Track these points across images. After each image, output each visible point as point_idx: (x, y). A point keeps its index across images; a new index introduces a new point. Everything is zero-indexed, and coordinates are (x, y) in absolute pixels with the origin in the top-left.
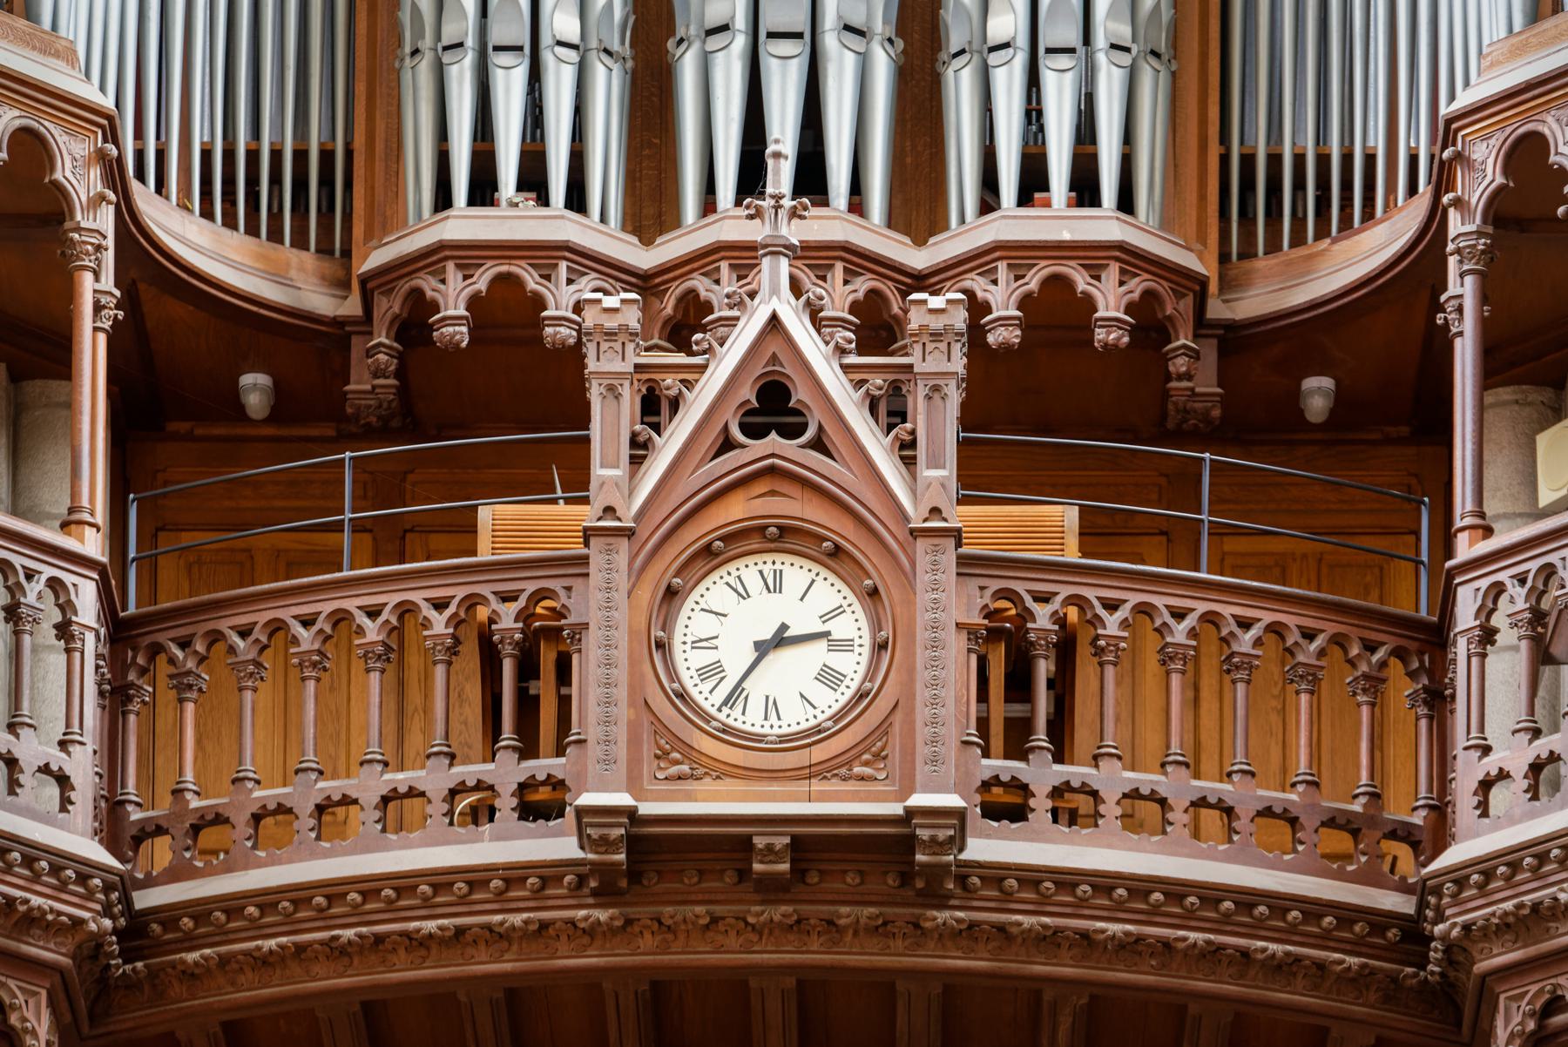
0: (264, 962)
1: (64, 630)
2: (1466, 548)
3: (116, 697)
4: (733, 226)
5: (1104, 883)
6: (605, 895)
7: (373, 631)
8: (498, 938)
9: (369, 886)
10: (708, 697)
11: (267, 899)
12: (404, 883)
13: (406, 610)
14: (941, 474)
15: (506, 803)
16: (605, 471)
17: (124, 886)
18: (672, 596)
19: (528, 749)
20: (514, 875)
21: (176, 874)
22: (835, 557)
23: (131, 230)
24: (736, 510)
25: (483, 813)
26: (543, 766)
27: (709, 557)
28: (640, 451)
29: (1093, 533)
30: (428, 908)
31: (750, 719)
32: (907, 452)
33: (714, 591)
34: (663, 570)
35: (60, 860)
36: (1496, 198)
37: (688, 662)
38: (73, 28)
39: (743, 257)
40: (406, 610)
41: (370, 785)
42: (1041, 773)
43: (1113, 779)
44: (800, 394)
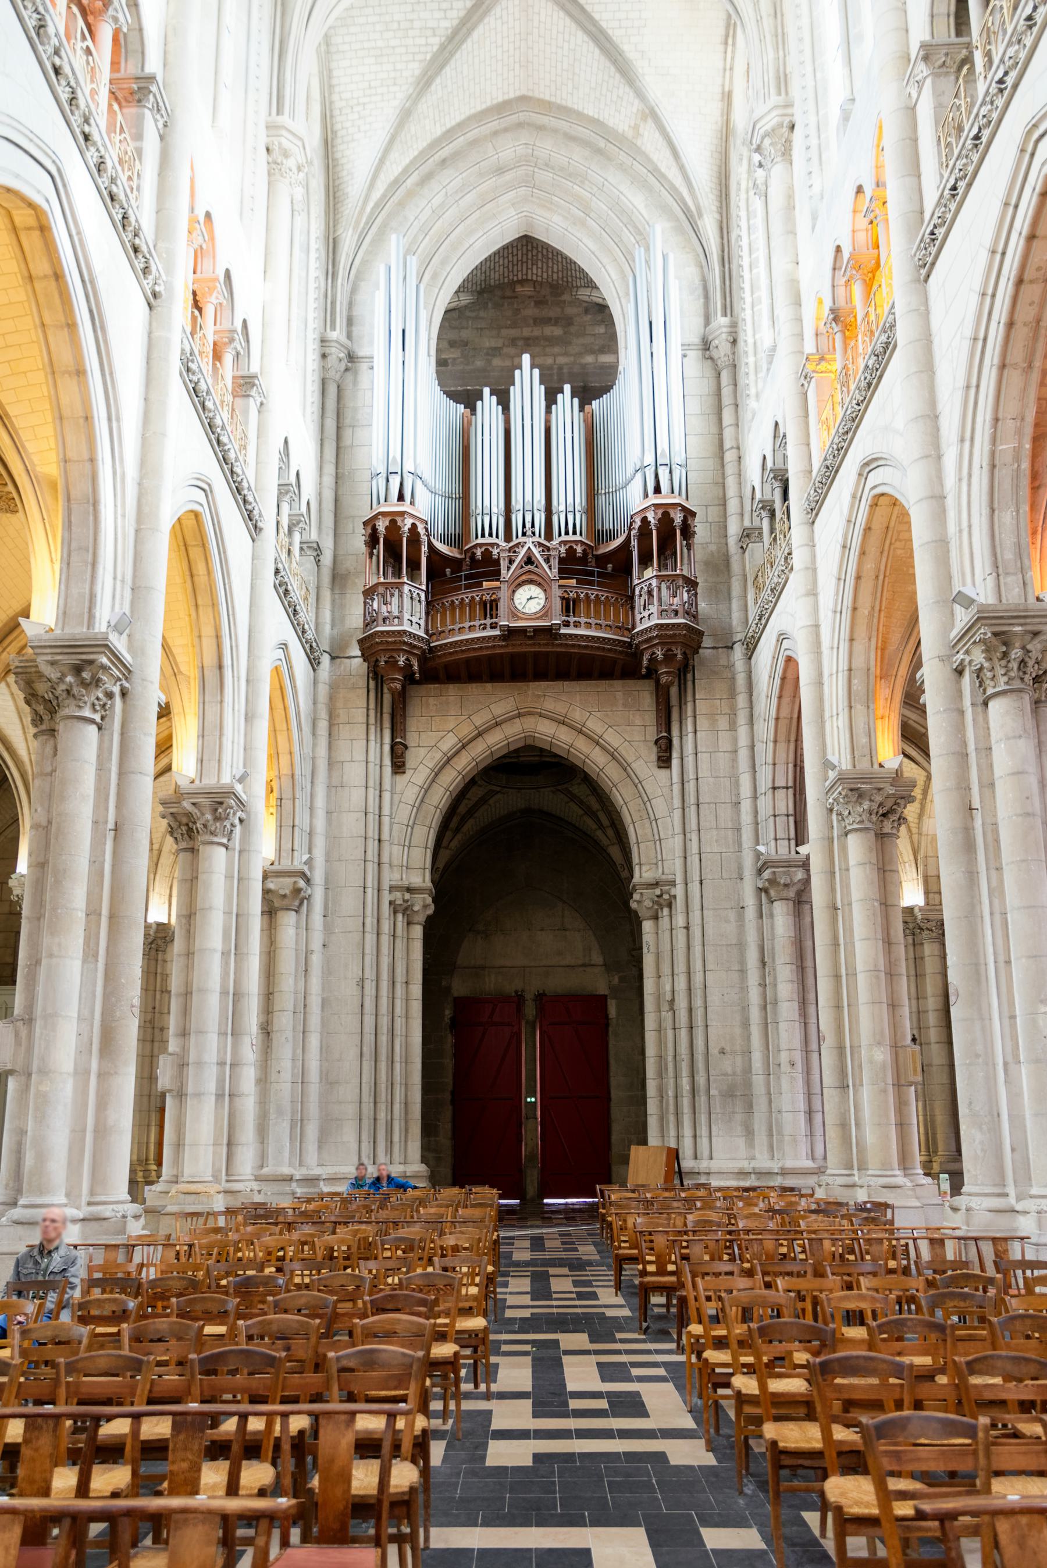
0: (451, 654)
1: (420, 601)
2: (636, 582)
3: (427, 614)
5: (582, 636)
6: (504, 640)
7: (467, 601)
8: (487, 648)
9: (467, 640)
10: (520, 607)
11: (451, 643)
12: (472, 639)
13: (473, 597)
14: (555, 571)
15: (488, 626)
16: (503, 572)
17: (428, 642)
18: (514, 591)
19: (491, 618)
20: (490, 637)
21: (437, 640)
22: (539, 585)
24: (524, 578)
25: (485, 628)
26: (494, 620)
27: (520, 585)
28: (509, 568)
30: (476, 643)
31: (526, 611)
32: (550, 567)
34: (513, 587)
35: (419, 636)
36: (640, 527)
37: (517, 602)
38: (421, 509)
40: (473, 597)
41: (467, 625)
42: (572, 619)
43: (583, 620)
44: (533, 559)
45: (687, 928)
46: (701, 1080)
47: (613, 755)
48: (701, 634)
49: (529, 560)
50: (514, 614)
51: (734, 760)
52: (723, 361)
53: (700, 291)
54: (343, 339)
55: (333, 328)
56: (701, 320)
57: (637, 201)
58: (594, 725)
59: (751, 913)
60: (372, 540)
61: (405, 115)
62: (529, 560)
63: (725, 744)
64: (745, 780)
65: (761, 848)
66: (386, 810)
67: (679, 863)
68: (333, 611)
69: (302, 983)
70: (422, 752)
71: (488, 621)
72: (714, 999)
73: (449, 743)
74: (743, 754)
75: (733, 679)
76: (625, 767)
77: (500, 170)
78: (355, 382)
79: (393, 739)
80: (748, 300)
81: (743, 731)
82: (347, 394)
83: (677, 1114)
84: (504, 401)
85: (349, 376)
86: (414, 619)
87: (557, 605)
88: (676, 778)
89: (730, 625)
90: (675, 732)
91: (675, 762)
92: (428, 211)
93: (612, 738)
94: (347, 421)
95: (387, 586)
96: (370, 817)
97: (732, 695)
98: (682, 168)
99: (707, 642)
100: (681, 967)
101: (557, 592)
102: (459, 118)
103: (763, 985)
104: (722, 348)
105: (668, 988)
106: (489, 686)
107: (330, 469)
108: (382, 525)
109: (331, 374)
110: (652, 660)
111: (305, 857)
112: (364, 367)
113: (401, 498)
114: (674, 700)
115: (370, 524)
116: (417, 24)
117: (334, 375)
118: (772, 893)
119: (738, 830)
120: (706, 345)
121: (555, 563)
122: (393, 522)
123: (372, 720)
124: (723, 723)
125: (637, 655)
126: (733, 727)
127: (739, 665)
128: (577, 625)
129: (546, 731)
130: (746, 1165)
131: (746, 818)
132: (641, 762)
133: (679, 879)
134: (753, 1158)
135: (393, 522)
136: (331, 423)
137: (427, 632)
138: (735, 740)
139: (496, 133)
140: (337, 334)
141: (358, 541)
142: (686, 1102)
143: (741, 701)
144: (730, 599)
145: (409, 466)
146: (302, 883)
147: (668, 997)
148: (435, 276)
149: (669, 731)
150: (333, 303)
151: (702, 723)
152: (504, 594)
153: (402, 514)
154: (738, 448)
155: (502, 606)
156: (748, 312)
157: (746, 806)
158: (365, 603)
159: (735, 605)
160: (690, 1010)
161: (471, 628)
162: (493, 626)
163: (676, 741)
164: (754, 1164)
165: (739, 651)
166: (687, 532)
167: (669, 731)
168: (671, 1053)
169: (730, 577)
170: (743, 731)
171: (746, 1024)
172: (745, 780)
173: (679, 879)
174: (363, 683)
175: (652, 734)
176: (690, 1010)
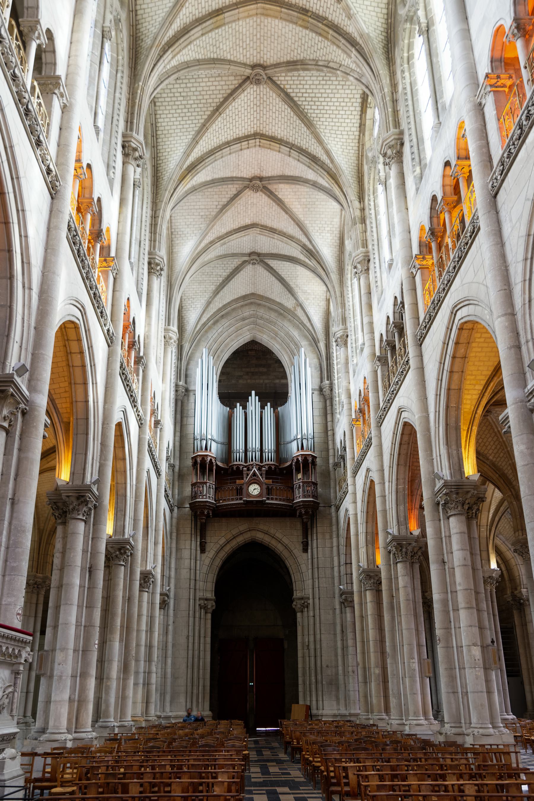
4: (251, 463)
22: (258, 484)
23: (216, 463)
27: (251, 484)
29: (273, 482)
33: (251, 486)
39: (252, 465)
42: (270, 497)
45: (314, 616)
46: (319, 677)
47: (286, 547)
48: (319, 503)
49: (254, 474)
50: (249, 495)
51: (332, 551)
52: (327, 397)
53: (319, 368)
54: (184, 384)
55: (180, 381)
56: (319, 380)
57: (295, 334)
58: (279, 535)
59: (338, 611)
60: (195, 464)
61: (209, 303)
62: (254, 474)
63: (328, 545)
64: (336, 559)
65: (341, 587)
66: (198, 568)
67: (311, 591)
68: (178, 490)
69: (165, 638)
70: (212, 544)
71: (239, 497)
72: (324, 645)
73: (222, 541)
74: (335, 549)
75: (331, 519)
76: (290, 551)
77: (244, 319)
78: (188, 400)
79: (201, 540)
80: (336, 376)
81: (335, 540)
82: (185, 404)
83: (310, 691)
84: (245, 407)
85: (186, 398)
86: (211, 496)
87: (265, 491)
88: (310, 557)
89: (330, 499)
90: (309, 539)
91: (309, 551)
92: (216, 334)
93: (285, 540)
94: (185, 415)
95: (201, 483)
96: (192, 571)
97: (331, 525)
98: (312, 325)
99: (321, 505)
100: (311, 632)
101: (265, 487)
102: (228, 301)
103: (342, 640)
104: (327, 391)
105: (307, 640)
106: (238, 518)
107: (178, 434)
108: (199, 460)
109: (179, 397)
110: (301, 513)
111: (168, 588)
112: (191, 394)
113: (206, 449)
114: (309, 527)
115: (194, 459)
116: (214, 273)
117: (180, 398)
118: (346, 604)
119: (333, 578)
120: (321, 390)
121: (264, 476)
122: (203, 459)
123: (193, 532)
124: (327, 536)
125: (295, 510)
126: (331, 538)
127: (334, 514)
128: (272, 499)
129: (260, 536)
130: (336, 712)
131: (336, 574)
132: (296, 550)
133: (311, 597)
134: (339, 709)
135: (203, 459)
136: (179, 416)
137: (215, 501)
138: (332, 543)
139: (242, 306)
140: (181, 383)
141: (190, 463)
142: (313, 687)
143: (334, 528)
144: (330, 488)
145: (209, 437)
146: (166, 598)
147: (307, 644)
148: (218, 357)
149: (307, 539)
150: (180, 370)
151: (320, 536)
152: (245, 487)
153: (207, 455)
154: (333, 430)
155: (244, 491)
156: (336, 381)
157: (336, 569)
158: (192, 489)
159: (332, 491)
160: (315, 649)
161: (233, 500)
162: (241, 499)
163: (310, 542)
164: (340, 712)
165: (333, 509)
166: (314, 463)
167: (307, 539)
168: (308, 666)
169: (330, 480)
170: (335, 540)
171: (336, 655)
172: (336, 559)
173: (311, 597)
174: (190, 518)
175: (301, 539)
176: (315, 649)
